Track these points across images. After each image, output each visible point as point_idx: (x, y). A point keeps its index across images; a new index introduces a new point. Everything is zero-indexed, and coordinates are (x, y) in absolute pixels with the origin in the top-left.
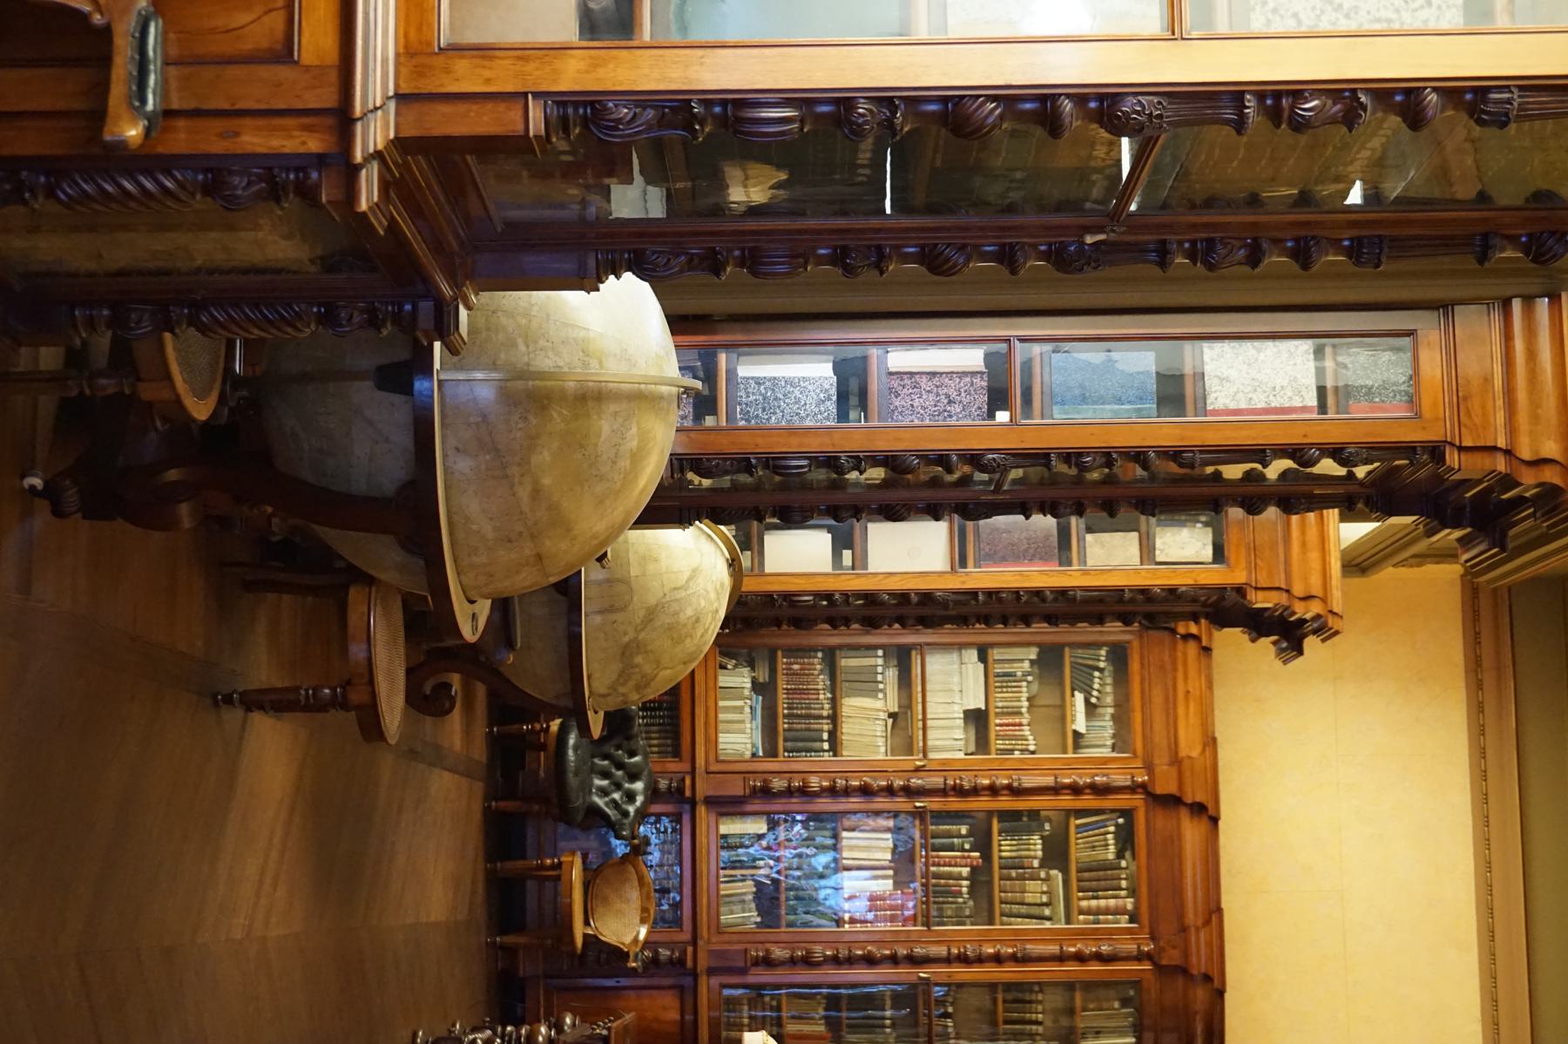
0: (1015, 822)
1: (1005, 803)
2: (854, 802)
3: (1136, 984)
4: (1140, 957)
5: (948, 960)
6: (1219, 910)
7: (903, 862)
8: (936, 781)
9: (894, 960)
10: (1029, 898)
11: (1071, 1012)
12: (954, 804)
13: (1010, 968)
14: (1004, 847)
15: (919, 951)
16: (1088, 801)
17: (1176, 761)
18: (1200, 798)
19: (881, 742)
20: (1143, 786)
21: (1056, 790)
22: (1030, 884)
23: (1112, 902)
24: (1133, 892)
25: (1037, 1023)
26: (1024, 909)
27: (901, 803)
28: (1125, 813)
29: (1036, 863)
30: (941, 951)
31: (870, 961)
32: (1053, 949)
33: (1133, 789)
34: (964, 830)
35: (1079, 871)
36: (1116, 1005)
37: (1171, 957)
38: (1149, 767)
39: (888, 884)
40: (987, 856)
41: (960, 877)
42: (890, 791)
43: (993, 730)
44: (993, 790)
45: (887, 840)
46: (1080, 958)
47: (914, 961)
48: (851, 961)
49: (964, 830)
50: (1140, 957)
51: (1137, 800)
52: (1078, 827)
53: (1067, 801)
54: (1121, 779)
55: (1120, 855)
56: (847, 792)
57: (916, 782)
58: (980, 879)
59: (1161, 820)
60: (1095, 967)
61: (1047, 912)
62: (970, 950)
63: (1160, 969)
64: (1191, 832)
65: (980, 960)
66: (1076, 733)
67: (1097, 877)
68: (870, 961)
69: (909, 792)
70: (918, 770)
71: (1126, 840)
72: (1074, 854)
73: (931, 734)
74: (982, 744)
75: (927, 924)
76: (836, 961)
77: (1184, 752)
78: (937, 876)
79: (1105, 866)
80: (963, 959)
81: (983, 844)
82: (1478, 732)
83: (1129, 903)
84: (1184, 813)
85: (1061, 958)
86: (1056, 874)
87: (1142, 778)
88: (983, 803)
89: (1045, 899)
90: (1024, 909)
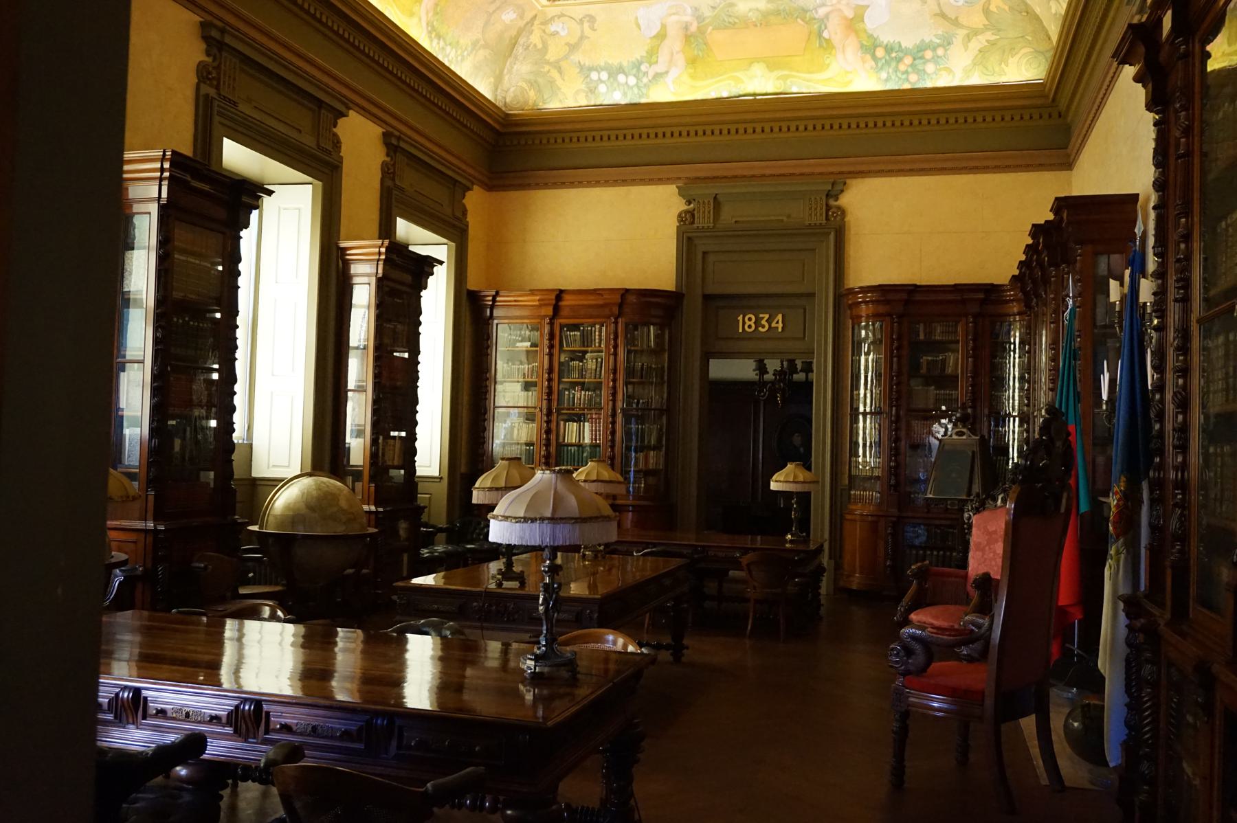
0: (564, 369)
1: (555, 376)
2: (553, 437)
3: (627, 325)
4: (616, 323)
5: (614, 401)
6: (595, 290)
7: (579, 418)
8: (545, 402)
9: (613, 423)
10: (594, 367)
11: (642, 351)
12: (555, 396)
13: (618, 376)
14: (575, 376)
16: (556, 342)
17: (540, 306)
18: (554, 297)
19: (531, 425)
20: (550, 319)
21: (551, 355)
22: (589, 367)
23: (597, 333)
24: (593, 325)
25: (643, 365)
26: (598, 369)
27: (554, 417)
28: (562, 327)
29: (581, 364)
30: (611, 403)
31: (613, 433)
32: (612, 358)
33: (551, 324)
34: (567, 393)
35: (584, 346)
36: (636, 333)
37: (616, 310)
38: (545, 316)
39: (586, 424)
40: (576, 384)
41: (585, 395)
42: (548, 422)
43: (530, 380)
44: (550, 380)
46: (616, 347)
47: (614, 415)
48: (613, 441)
49: (567, 393)
50: (616, 323)
51: (558, 322)
52: (567, 347)
53: (556, 351)
54: (547, 329)
55: (578, 329)
56: (548, 440)
57: (545, 411)
58: (583, 386)
59: (564, 312)
60: (619, 341)
61: (599, 360)
63: (620, 315)
64: (567, 301)
65: (614, 388)
66: (531, 346)
67: (586, 340)
68: (613, 433)
69: (549, 413)
70: (541, 411)
71: (575, 327)
73: (530, 405)
74: (534, 384)
75: (602, 408)
76: (613, 447)
77: (537, 303)
78: (584, 404)
79: (583, 335)
80: (614, 394)
81: (573, 385)
82: (546, 186)
84: (562, 303)
85: (615, 354)
87: (547, 320)
88: (555, 384)
89: (594, 361)
90: (598, 369)
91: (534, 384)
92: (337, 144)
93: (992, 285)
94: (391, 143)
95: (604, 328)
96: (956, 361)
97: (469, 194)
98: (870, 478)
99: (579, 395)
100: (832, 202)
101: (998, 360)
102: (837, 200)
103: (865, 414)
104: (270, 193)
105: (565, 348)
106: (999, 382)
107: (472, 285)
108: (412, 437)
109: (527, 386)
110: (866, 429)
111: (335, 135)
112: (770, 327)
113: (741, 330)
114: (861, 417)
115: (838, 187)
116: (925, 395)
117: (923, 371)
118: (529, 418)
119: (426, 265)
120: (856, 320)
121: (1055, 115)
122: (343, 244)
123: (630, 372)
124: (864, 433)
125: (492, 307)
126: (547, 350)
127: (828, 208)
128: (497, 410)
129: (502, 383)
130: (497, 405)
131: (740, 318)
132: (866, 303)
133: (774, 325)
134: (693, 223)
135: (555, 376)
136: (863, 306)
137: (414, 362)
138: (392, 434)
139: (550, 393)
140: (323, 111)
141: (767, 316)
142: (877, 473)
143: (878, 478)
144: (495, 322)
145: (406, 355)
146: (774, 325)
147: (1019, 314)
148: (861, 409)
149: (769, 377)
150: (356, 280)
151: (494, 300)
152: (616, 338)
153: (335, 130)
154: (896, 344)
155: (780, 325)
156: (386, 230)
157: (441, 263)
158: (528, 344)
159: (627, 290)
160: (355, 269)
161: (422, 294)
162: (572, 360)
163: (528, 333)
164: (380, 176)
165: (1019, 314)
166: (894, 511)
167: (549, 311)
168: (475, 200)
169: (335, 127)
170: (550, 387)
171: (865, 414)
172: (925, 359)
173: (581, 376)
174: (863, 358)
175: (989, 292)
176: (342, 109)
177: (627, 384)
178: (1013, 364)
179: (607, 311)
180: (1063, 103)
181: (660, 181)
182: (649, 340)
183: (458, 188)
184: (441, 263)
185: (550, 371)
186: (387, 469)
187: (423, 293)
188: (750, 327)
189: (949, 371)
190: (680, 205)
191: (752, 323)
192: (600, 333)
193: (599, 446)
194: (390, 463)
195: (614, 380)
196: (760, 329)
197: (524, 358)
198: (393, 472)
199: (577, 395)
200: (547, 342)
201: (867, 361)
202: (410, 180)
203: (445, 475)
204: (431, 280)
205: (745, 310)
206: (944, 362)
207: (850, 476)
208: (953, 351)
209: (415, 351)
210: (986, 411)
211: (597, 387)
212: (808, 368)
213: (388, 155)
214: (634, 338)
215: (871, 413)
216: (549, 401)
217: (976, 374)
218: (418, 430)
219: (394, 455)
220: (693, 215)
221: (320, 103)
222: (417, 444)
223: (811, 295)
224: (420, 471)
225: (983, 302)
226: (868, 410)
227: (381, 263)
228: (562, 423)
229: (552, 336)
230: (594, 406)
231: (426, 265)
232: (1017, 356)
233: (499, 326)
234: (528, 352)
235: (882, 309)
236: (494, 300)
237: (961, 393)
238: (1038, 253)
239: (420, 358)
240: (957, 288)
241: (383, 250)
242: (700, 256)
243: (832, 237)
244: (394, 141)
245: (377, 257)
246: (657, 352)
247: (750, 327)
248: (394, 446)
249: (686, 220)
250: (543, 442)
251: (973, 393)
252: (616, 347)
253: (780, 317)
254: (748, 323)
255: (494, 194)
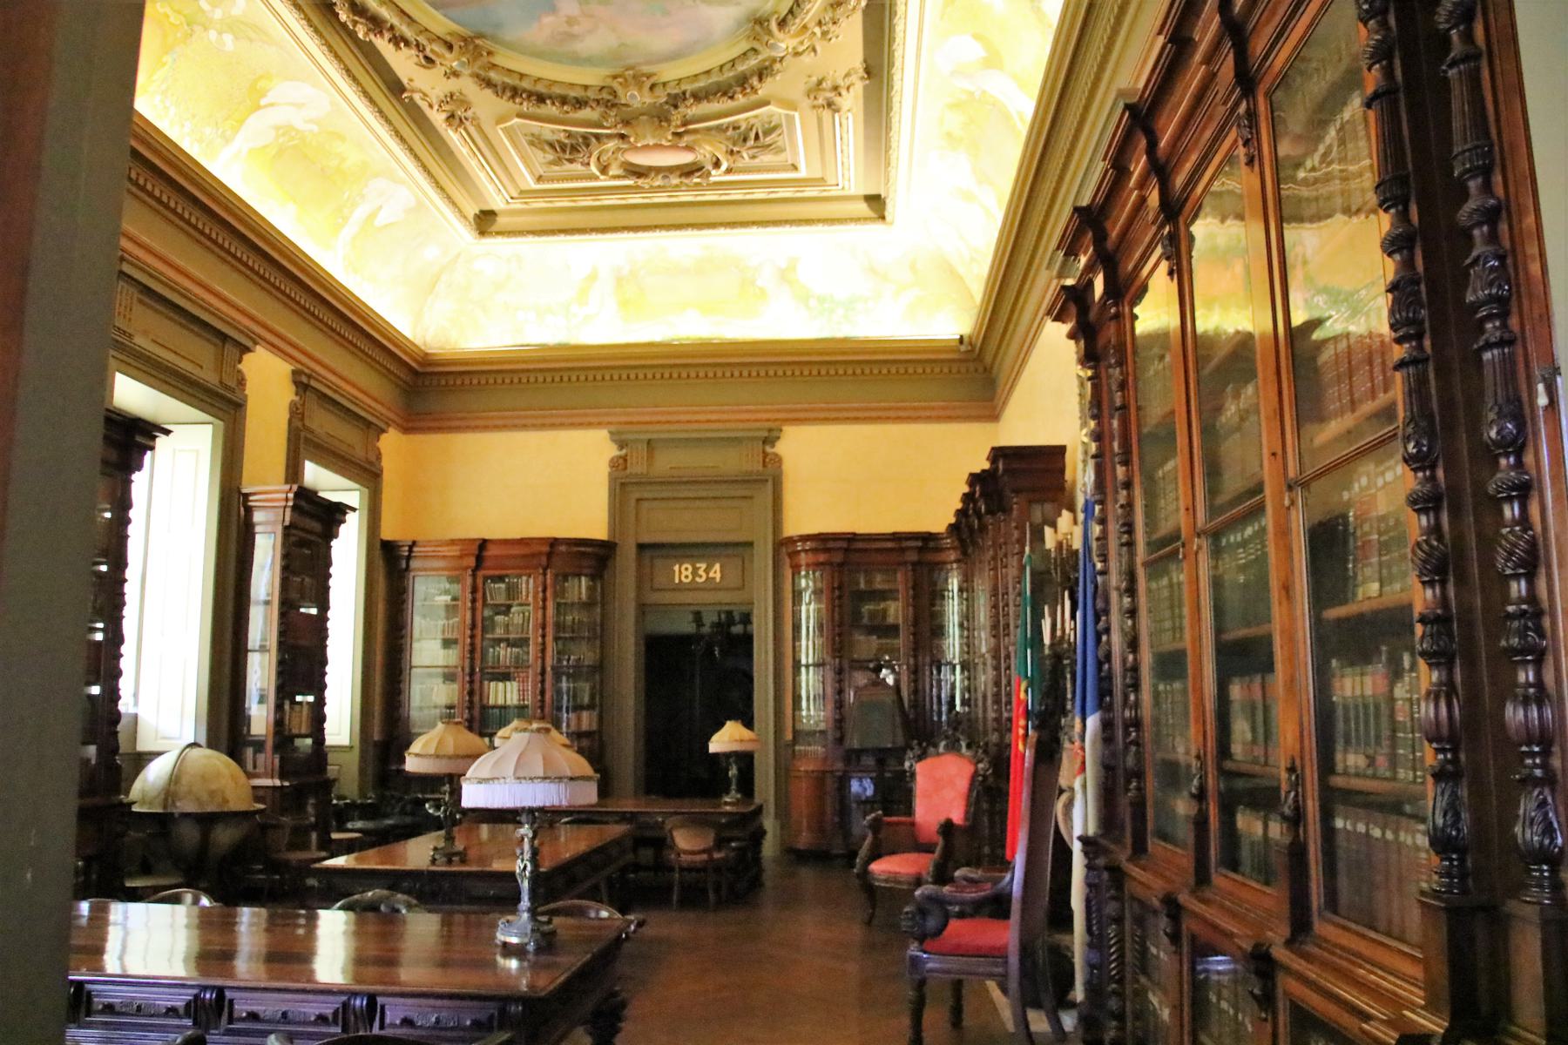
0: (488, 625)
1: (478, 631)
2: (476, 699)
3: (556, 576)
4: (545, 574)
5: (543, 659)
6: (522, 539)
7: (505, 677)
8: (467, 662)
9: (543, 682)
11: (573, 604)
12: (478, 655)
14: (499, 632)
15: (539, 670)
16: (479, 595)
17: (461, 557)
21: (473, 609)
24: (519, 576)
27: (477, 677)
30: (540, 661)
31: (543, 693)
32: (540, 613)
33: (474, 576)
37: (544, 560)
38: (466, 568)
42: (471, 682)
43: (450, 636)
44: (472, 637)
45: (493, 684)
46: (544, 600)
47: (543, 673)
48: (543, 701)
51: (481, 574)
52: (492, 599)
53: (479, 605)
54: (469, 581)
55: (504, 582)
56: (471, 702)
57: (467, 670)
58: (511, 643)
59: (488, 563)
60: (549, 594)
62: (540, 648)
64: (492, 551)
67: (512, 592)
68: (543, 693)
69: (472, 673)
71: (501, 579)
72: (502, 602)
74: (455, 642)
76: (542, 708)
77: (458, 553)
79: (508, 589)
80: (543, 651)
81: (498, 641)
83: (524, 578)
84: (486, 554)
85: (544, 608)
86: (513, 610)
87: (470, 572)
88: (478, 640)
91: (455, 642)
92: (241, 382)
93: (930, 534)
94: (302, 383)
95: (531, 581)
96: (896, 611)
97: (384, 437)
98: (812, 733)
99: (505, 654)
100: (769, 449)
101: (937, 608)
102: (773, 446)
103: (807, 666)
104: (167, 432)
105: (489, 601)
106: (939, 631)
107: (387, 533)
108: (320, 702)
109: (447, 643)
110: (809, 681)
111: (239, 371)
112: (708, 578)
113: (677, 581)
114: (803, 670)
115: (775, 434)
116: (866, 645)
117: (865, 621)
118: (449, 677)
119: (334, 514)
120: (796, 569)
121: (981, 369)
122: (245, 491)
123: (559, 627)
124: (808, 685)
125: (409, 558)
126: (469, 605)
127: (765, 454)
128: (414, 670)
129: (419, 640)
130: (413, 664)
131: (676, 568)
132: (806, 551)
133: (711, 575)
134: (626, 468)
135: (478, 631)
136: (803, 555)
137: (322, 618)
138: (299, 698)
139: (472, 651)
140: (227, 346)
141: (703, 566)
142: (822, 726)
143: (821, 732)
144: (412, 574)
145: (314, 611)
146: (711, 575)
147: (955, 561)
148: (804, 661)
149: (706, 630)
150: (258, 529)
151: (410, 551)
152: (544, 591)
153: (240, 366)
154: (837, 593)
155: (718, 576)
156: (293, 472)
157: (354, 510)
158: (448, 598)
159: (556, 539)
160: (258, 517)
161: (332, 543)
162: (498, 614)
163: (448, 586)
164: (287, 416)
165: (955, 561)
166: (839, 765)
167: (472, 562)
168: (391, 444)
169: (240, 362)
170: (472, 644)
171: (807, 666)
172: (867, 608)
173: (507, 631)
174: (804, 608)
175: (927, 540)
176: (249, 344)
177: (556, 639)
178: (953, 610)
179: (535, 562)
180: (988, 359)
181: (589, 425)
182: (580, 593)
183: (372, 429)
184: (354, 510)
185: (473, 626)
186: (292, 738)
187: (334, 543)
188: (687, 577)
189: (891, 620)
190: (613, 451)
191: (689, 573)
192: (528, 586)
193: (527, 707)
194: (295, 731)
195: (544, 636)
196: (698, 579)
197: (443, 613)
198: (298, 742)
199: (502, 653)
200: (469, 596)
201: (809, 611)
202: (323, 423)
203: (357, 743)
204: (343, 528)
205: (681, 559)
206: (885, 611)
207: (796, 733)
208: (896, 599)
209: (324, 606)
210: (928, 659)
211: (522, 643)
212: (746, 619)
213: (297, 394)
214: (563, 591)
215: (817, 665)
216: (472, 659)
217: (916, 623)
218: (327, 693)
219: (299, 723)
220: (625, 460)
221: (224, 337)
222: (326, 709)
223: (750, 544)
224: (330, 740)
225: (920, 550)
226: (811, 661)
227: (288, 511)
228: (486, 683)
229: (474, 590)
230: (520, 664)
231: (334, 514)
232: (956, 602)
233: (417, 579)
234: (447, 606)
235: (822, 558)
236: (410, 551)
237: (902, 641)
238: (975, 502)
239: (330, 614)
240: (896, 537)
241: (291, 495)
242: (633, 503)
243: (770, 484)
244: (304, 379)
245: (283, 504)
246: (588, 605)
247: (687, 577)
248: (301, 712)
249: (618, 465)
250: (466, 704)
251: (916, 643)
252: (544, 600)
253: (717, 567)
254: (684, 573)
255: (412, 437)
